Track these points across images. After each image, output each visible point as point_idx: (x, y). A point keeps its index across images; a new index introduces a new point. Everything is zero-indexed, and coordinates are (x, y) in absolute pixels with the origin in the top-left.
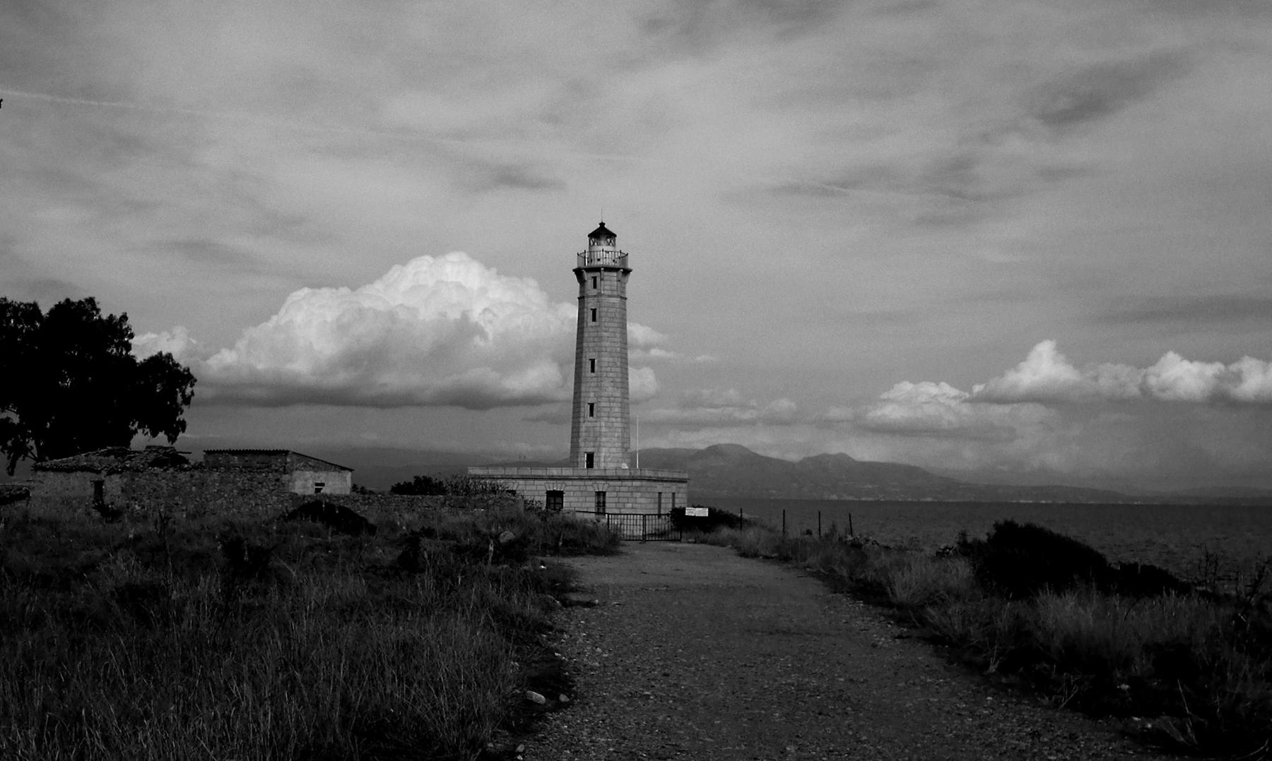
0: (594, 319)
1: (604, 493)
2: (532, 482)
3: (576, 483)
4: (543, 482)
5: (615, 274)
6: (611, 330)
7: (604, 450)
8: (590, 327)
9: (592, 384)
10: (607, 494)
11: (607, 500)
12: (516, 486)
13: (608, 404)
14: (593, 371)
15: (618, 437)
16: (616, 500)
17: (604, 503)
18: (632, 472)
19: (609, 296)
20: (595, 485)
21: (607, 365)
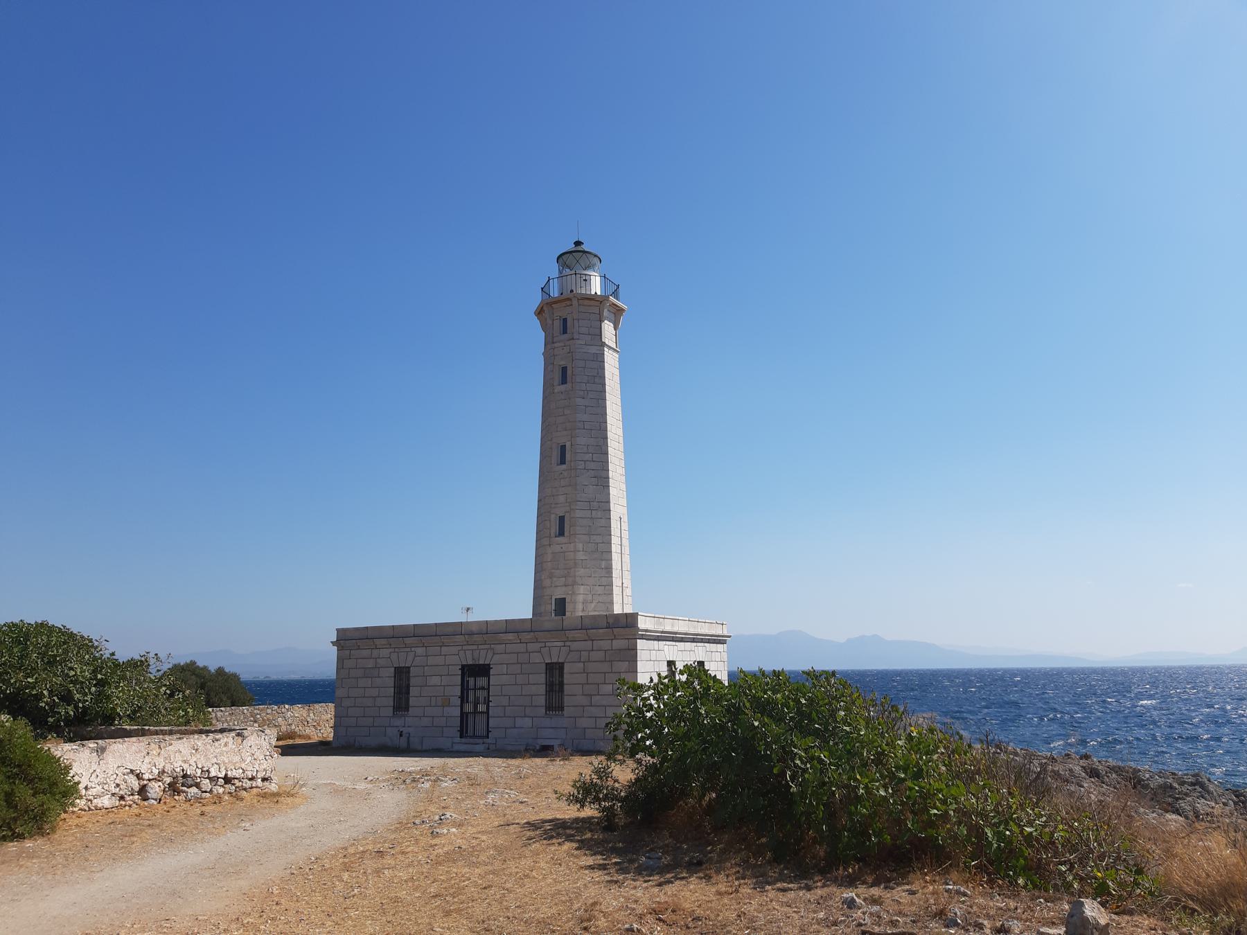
1: (560, 666)
11: (567, 678)
12: (410, 658)
13: (588, 514)
17: (561, 684)
20: (545, 650)
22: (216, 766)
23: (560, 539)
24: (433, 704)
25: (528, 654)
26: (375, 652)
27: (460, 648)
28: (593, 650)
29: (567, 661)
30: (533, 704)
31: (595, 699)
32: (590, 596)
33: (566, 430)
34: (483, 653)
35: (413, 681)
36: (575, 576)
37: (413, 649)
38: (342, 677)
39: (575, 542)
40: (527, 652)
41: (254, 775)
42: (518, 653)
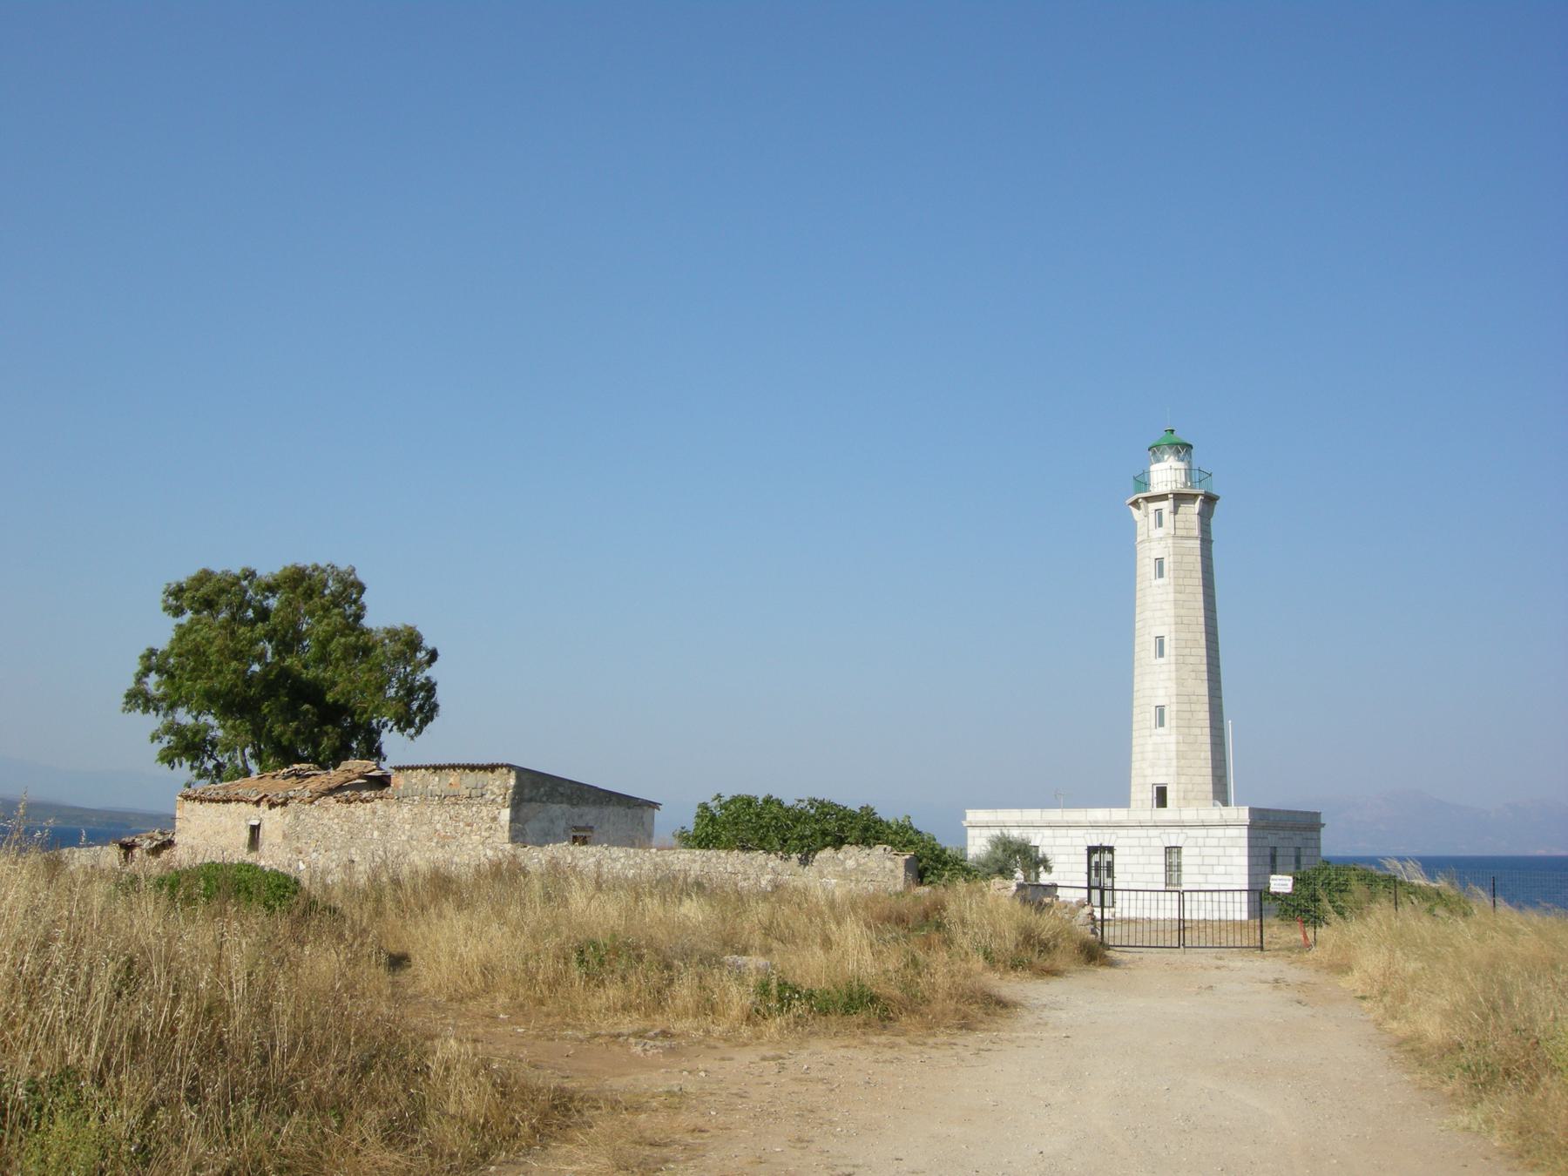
2: (1063, 831)
3: (1132, 832)
4: (1081, 832)
10: (1184, 851)
11: (1184, 860)
16: (1199, 860)
17: (1179, 865)
23: (1160, 730)
33: (1164, 624)
34: (1107, 836)
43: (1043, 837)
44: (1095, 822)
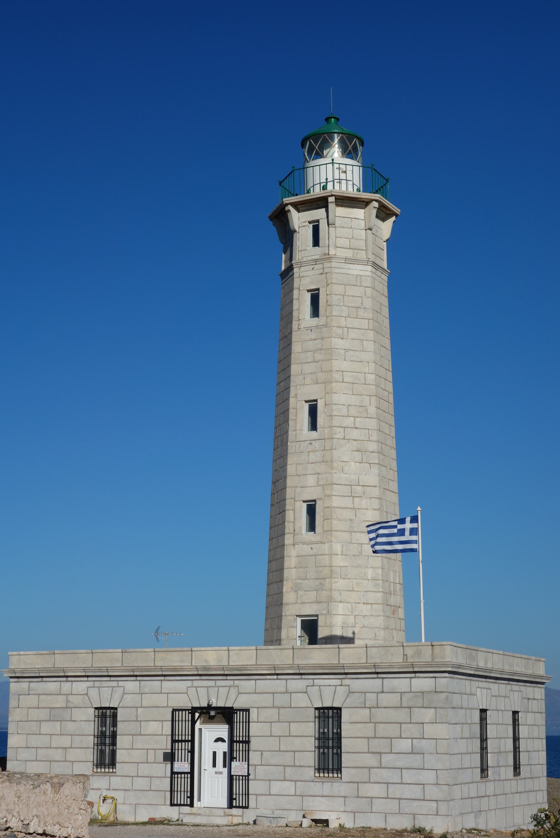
0: (315, 312)
2: (155, 684)
5: (359, 213)
6: (353, 334)
7: (340, 608)
8: (307, 329)
9: (313, 457)
11: (346, 730)
13: (348, 502)
14: (313, 426)
15: (374, 579)
16: (368, 730)
17: (338, 737)
18: (409, 652)
19: (347, 261)
20: (313, 691)
21: (344, 412)
22: (35, 820)
24: (151, 759)
25: (287, 695)
26: (66, 686)
27: (189, 683)
28: (383, 692)
29: (310, 706)
30: (297, 764)
31: (387, 759)
32: (352, 617)
33: (317, 383)
35: (121, 727)
36: (331, 590)
37: (121, 684)
38: (18, 719)
39: (331, 541)
40: (287, 692)
41: (69, 833)
42: (273, 693)
43: (124, 694)
44: (205, 668)
